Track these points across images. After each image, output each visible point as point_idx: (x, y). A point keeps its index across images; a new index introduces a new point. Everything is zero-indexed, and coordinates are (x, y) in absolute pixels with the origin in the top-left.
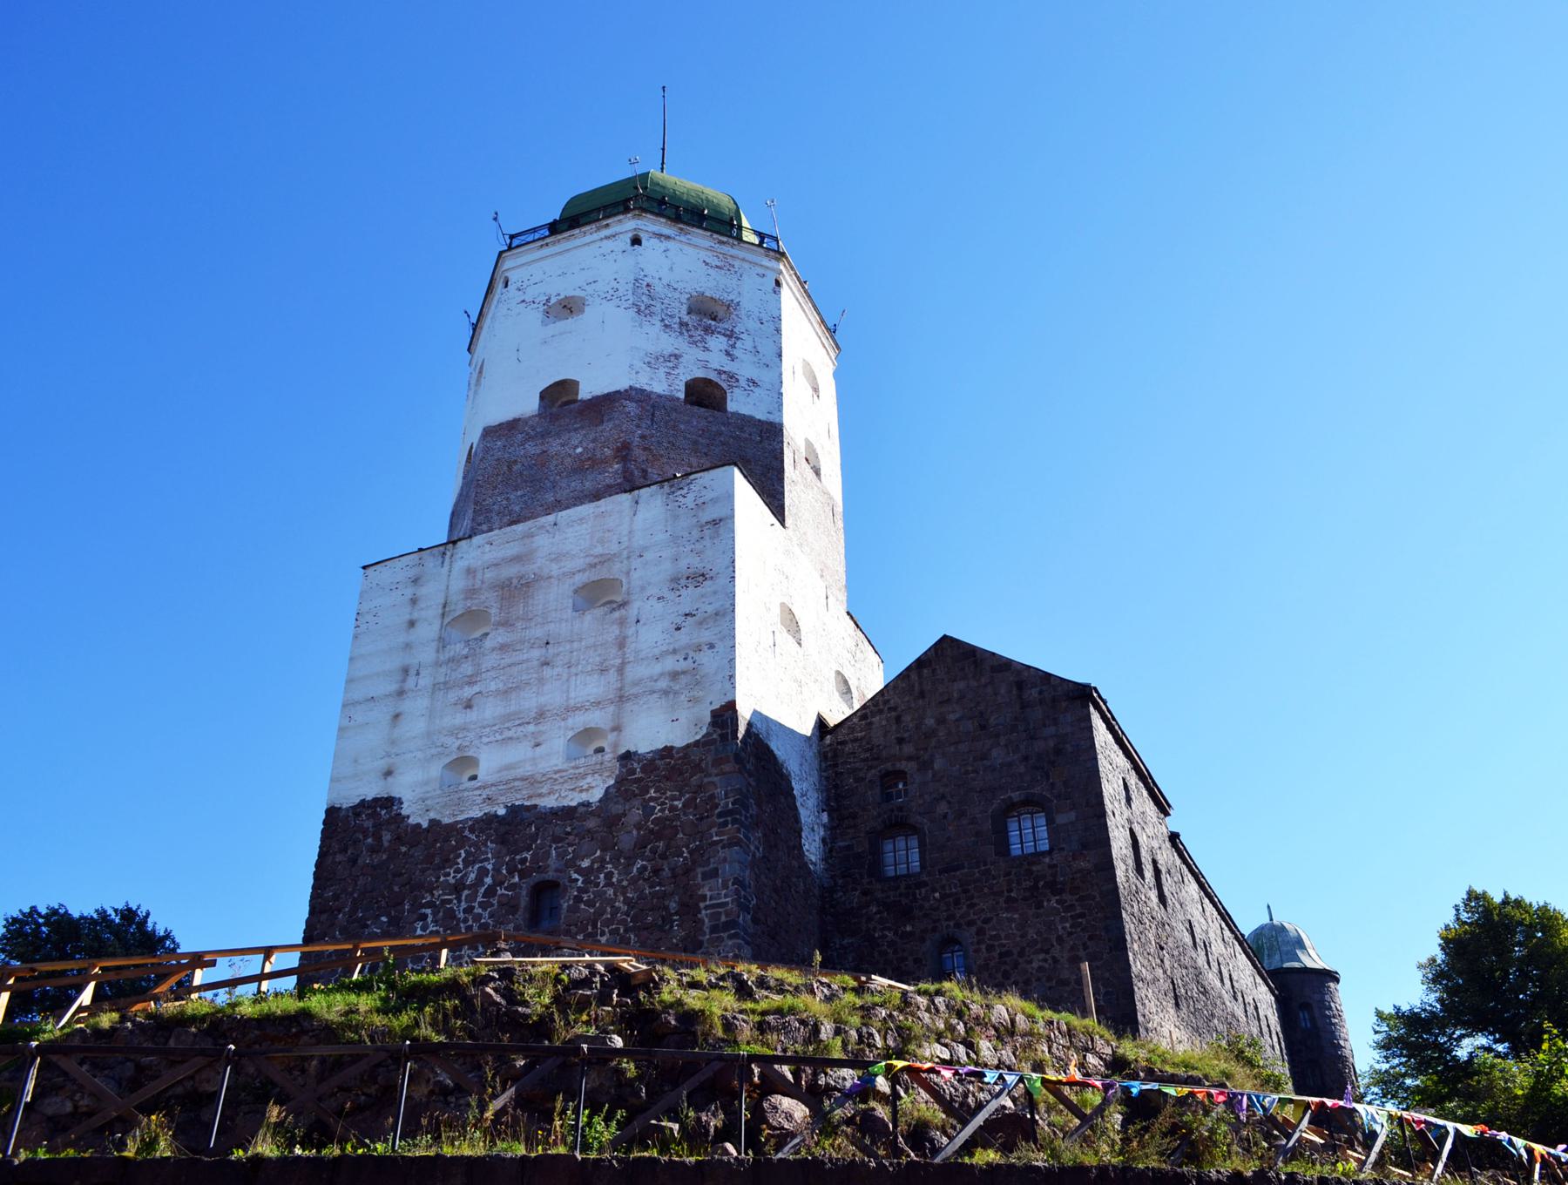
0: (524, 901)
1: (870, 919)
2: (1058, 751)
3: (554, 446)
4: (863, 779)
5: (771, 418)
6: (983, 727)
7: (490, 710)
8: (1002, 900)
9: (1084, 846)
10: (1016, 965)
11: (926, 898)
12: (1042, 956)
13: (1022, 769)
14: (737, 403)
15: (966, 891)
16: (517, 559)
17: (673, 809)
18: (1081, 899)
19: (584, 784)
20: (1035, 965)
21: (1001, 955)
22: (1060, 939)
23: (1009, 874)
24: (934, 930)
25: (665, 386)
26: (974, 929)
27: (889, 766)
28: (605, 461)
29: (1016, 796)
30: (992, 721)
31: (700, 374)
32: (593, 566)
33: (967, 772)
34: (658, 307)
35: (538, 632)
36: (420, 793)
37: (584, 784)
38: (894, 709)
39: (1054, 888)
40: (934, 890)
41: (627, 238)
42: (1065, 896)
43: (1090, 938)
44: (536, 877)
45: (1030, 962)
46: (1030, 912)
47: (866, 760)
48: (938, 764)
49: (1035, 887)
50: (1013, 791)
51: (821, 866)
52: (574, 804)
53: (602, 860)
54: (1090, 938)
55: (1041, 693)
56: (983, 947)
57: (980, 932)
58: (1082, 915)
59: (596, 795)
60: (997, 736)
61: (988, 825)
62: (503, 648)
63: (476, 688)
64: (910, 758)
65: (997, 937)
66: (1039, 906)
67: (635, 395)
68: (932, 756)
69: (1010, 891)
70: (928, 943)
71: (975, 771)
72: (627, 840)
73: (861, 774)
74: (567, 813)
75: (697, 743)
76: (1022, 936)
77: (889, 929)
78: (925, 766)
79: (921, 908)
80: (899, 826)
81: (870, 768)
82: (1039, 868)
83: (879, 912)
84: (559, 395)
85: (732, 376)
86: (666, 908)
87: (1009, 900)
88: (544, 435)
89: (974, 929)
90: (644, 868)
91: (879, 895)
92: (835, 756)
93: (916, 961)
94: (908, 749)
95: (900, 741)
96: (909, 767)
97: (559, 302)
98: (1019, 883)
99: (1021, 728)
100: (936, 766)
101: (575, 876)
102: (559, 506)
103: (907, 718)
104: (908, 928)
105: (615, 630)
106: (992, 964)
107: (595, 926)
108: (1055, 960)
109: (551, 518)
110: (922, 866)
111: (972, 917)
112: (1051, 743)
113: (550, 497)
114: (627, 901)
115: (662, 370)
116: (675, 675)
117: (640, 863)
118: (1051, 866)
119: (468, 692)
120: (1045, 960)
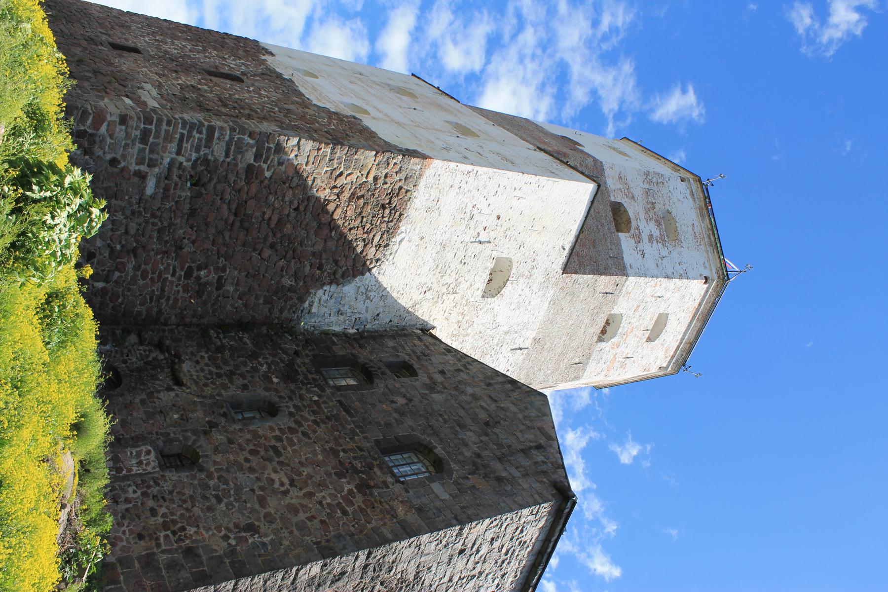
1: (274, 356)
2: (499, 479)
5: (629, 271)
6: (487, 424)
8: (332, 445)
9: (420, 510)
10: (270, 460)
11: (309, 391)
12: (286, 481)
13: (468, 454)
20: (274, 476)
21: (274, 448)
22: (310, 495)
23: (361, 450)
27: (416, 366)
29: (439, 450)
30: (497, 431)
33: (441, 416)
38: (466, 368)
39: (364, 487)
40: (319, 396)
42: (359, 499)
43: (322, 522)
45: (275, 471)
46: (329, 468)
47: (414, 352)
49: (357, 472)
50: (444, 449)
54: (322, 522)
55: (544, 462)
56: (278, 433)
57: (292, 430)
58: (345, 513)
60: (487, 435)
65: (292, 444)
66: (340, 475)
68: (442, 393)
69: (344, 451)
70: (267, 394)
71: (445, 421)
77: (269, 367)
78: (432, 387)
79: (300, 389)
80: (367, 375)
81: (409, 355)
82: (379, 473)
83: (282, 361)
87: (335, 453)
89: (293, 425)
92: (405, 335)
93: (245, 387)
94: (439, 378)
95: (442, 372)
96: (423, 378)
98: (355, 458)
99: (503, 450)
100: (434, 395)
103: (463, 376)
104: (275, 380)
106: (262, 441)
108: (287, 491)
110: (339, 388)
111: (306, 424)
112: (504, 474)
115: (621, 186)
118: (385, 484)
120: (282, 484)
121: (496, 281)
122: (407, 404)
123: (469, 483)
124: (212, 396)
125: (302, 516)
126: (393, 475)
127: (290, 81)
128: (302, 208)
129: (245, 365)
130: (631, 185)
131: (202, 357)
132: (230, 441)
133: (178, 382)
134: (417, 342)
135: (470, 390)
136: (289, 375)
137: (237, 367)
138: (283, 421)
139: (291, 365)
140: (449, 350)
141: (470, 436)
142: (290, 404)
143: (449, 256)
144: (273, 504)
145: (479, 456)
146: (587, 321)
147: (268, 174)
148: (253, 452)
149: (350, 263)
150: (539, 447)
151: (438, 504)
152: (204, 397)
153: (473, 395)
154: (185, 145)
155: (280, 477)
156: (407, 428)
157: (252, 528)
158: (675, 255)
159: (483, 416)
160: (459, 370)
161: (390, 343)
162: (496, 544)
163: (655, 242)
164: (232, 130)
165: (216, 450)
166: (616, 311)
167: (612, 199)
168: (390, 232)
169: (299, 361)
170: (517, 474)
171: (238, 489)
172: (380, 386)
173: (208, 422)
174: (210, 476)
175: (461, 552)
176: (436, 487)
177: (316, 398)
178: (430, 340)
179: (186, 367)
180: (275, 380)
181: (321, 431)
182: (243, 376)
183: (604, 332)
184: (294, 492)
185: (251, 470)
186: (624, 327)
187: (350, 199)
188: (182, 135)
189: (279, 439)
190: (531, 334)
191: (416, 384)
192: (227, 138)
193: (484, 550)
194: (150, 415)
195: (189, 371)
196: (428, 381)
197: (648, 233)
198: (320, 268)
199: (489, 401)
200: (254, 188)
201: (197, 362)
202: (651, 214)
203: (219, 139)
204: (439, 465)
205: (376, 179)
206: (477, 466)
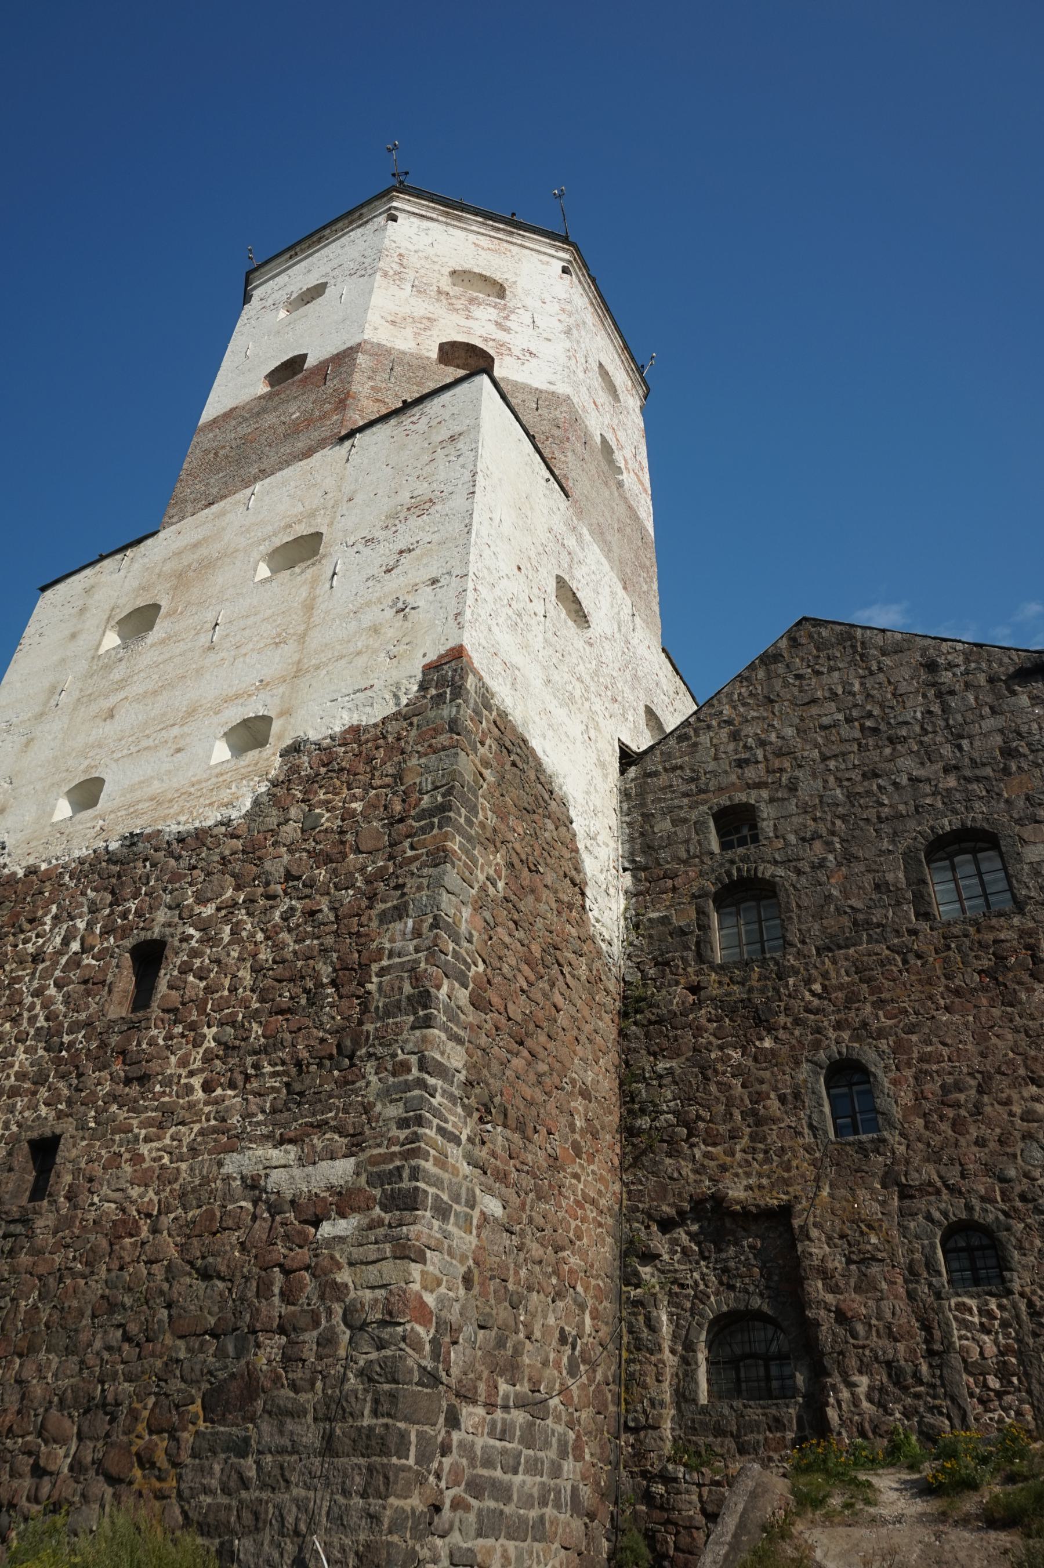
1: (699, 1031)
4: (685, 821)
5: (562, 389)
7: (129, 717)
15: (868, 981)
35: (210, 616)
37: (225, 795)
38: (729, 722)
40: (808, 981)
47: (686, 795)
52: (210, 823)
56: (908, 1073)
62: (163, 642)
63: (121, 695)
64: (759, 785)
73: (682, 814)
74: (198, 839)
76: (983, 1055)
90: (292, 909)
91: (715, 991)
92: (641, 795)
95: (741, 764)
101: (191, 931)
103: (749, 730)
104: (767, 1044)
105: (304, 592)
107: (202, 1011)
113: (254, 470)
114: (257, 970)
116: (375, 630)
119: (113, 700)
122: (828, 844)
127: (132, 840)
128: (516, 917)
131: (707, 1155)
142: (831, 1034)
147: (481, 967)
152: (817, 1179)
154: (449, 1127)
160: (735, 736)
161: (663, 826)
163: (508, 323)
167: (434, 354)
168: (539, 767)
173: (884, 1186)
177: (817, 987)
178: (657, 757)
179: (737, 1192)
180: (767, 1044)
182: (758, 1098)
188: (441, 1130)
191: (767, 812)
192: (443, 1036)
194: (865, 1286)
195: (749, 1188)
196: (765, 794)
198: (570, 906)
201: (723, 1168)
203: (442, 1053)
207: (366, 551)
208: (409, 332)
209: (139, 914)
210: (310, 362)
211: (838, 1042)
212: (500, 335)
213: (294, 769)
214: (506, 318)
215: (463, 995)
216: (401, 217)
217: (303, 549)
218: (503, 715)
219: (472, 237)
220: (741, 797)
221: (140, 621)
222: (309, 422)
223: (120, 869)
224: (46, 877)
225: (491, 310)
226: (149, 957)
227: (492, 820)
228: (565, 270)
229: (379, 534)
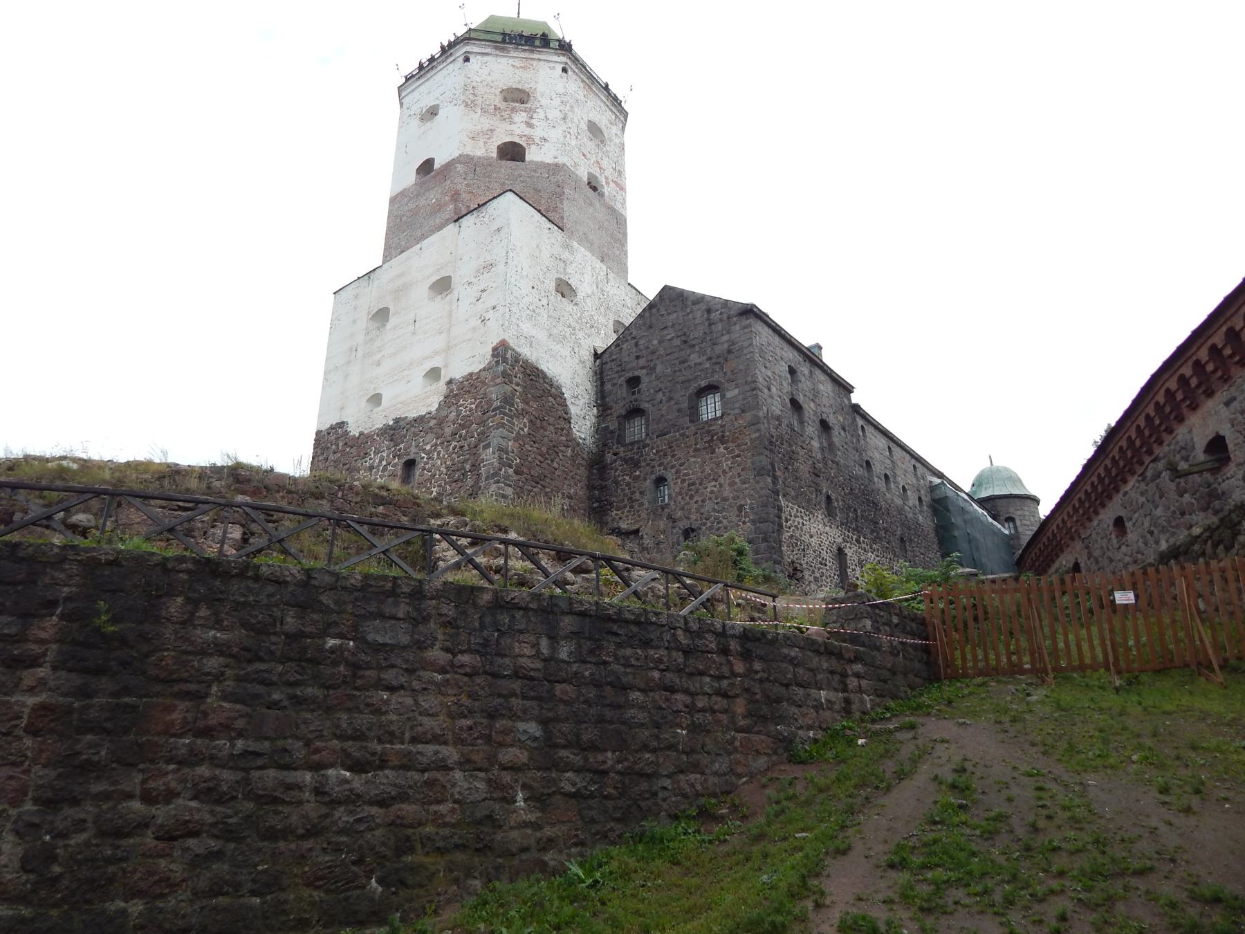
0: (399, 472)
2: (729, 352)
3: (422, 202)
5: (561, 160)
9: (743, 411)
11: (648, 454)
14: (532, 155)
16: (402, 275)
17: (471, 410)
18: (739, 446)
19: (429, 401)
21: (689, 485)
24: (652, 473)
25: (483, 151)
26: (673, 471)
27: (630, 375)
28: (446, 204)
29: (703, 383)
31: (508, 139)
32: (438, 270)
34: (479, 102)
35: (412, 316)
36: (360, 420)
37: (429, 401)
39: (723, 440)
41: (461, 59)
42: (730, 445)
44: (406, 458)
48: (659, 368)
49: (712, 440)
51: (589, 441)
53: (436, 445)
59: (434, 408)
60: (694, 346)
61: (685, 405)
64: (642, 368)
65: (687, 474)
67: (464, 160)
72: (448, 431)
74: (420, 420)
75: (484, 369)
80: (635, 412)
84: (426, 167)
85: (530, 138)
86: (464, 468)
87: (696, 450)
88: (418, 195)
89: (673, 471)
91: (622, 454)
92: (601, 373)
93: (641, 493)
94: (642, 362)
95: (638, 357)
97: (428, 111)
102: (424, 237)
103: (642, 342)
108: (721, 485)
109: (419, 246)
112: (726, 346)
116: (474, 329)
117: (454, 443)
118: (722, 426)
119: (378, 356)
121: (565, 289)
123: (729, 373)
124: (648, 514)
125: (737, 480)
126: (716, 419)
127: (397, 421)
129: (623, 490)
130: (478, 128)
132: (683, 509)
133: (636, 532)
134: (608, 366)
135: (655, 342)
136: (636, 464)
137: (625, 495)
138: (670, 475)
139: (625, 461)
140: (617, 344)
141: (695, 358)
143: (555, 331)
144: (726, 494)
145: (710, 358)
146: (591, 210)
148: (691, 497)
149: (560, 408)
150: (709, 311)
151: (740, 397)
153: (660, 342)
155: (710, 486)
156: (683, 397)
157: (740, 508)
158: (544, 101)
159: (677, 342)
160: (636, 345)
161: (608, 387)
162: (768, 365)
164: (498, 482)
165: (688, 518)
166: (585, 180)
167: (495, 155)
168: (545, 376)
169: (622, 454)
170: (726, 338)
171: (714, 510)
172: (644, 405)
174: (705, 524)
175: (769, 389)
176: (729, 395)
178: (606, 355)
181: (679, 453)
182: (634, 493)
183: (595, 189)
184: (721, 480)
185: (703, 501)
186: (595, 171)
187: (527, 404)
189: (683, 481)
190: (598, 264)
193: (769, 374)
194: (659, 551)
196: (644, 371)
197: (523, 126)
198: (562, 429)
199: (665, 332)
200: (525, 470)
202: (506, 115)
204: (712, 388)
205: (518, 385)
206: (719, 361)
207: (469, 289)
208: (481, 143)
209: (405, 449)
210: (437, 166)
211: (659, 471)
212: (528, 131)
213: (452, 391)
214: (531, 118)
215: (511, 471)
216: (471, 57)
217: (443, 286)
218: (526, 362)
219: (511, 61)
220: (637, 373)
221: (382, 315)
222: (440, 207)
223: (395, 431)
224: (369, 436)
225: (524, 114)
226: (410, 464)
227: (521, 406)
228: (564, 70)
229: (473, 280)
